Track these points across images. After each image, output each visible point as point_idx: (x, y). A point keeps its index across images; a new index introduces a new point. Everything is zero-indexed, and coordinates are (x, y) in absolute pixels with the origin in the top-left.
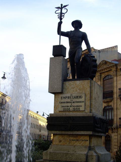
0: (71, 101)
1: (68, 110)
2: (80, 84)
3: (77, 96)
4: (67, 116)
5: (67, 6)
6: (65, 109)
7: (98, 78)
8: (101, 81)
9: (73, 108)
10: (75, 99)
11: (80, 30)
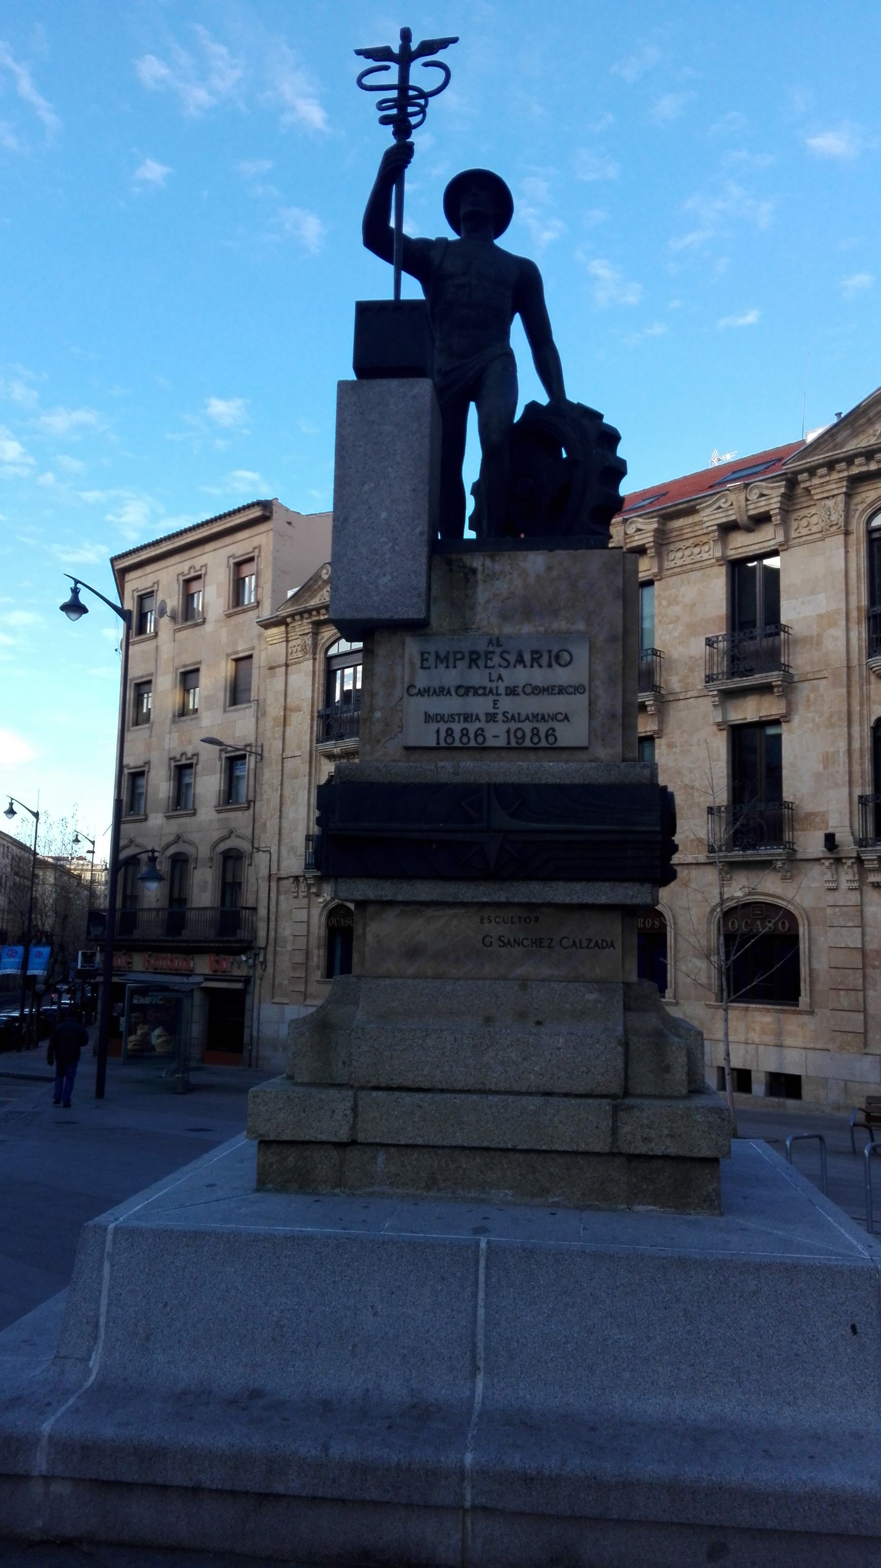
0: (493, 685)
1: (473, 744)
2: (555, 573)
3: (534, 652)
4: (471, 779)
7: (304, 649)
8: (314, 659)
9: (504, 727)
10: (520, 667)
11: (500, 242)
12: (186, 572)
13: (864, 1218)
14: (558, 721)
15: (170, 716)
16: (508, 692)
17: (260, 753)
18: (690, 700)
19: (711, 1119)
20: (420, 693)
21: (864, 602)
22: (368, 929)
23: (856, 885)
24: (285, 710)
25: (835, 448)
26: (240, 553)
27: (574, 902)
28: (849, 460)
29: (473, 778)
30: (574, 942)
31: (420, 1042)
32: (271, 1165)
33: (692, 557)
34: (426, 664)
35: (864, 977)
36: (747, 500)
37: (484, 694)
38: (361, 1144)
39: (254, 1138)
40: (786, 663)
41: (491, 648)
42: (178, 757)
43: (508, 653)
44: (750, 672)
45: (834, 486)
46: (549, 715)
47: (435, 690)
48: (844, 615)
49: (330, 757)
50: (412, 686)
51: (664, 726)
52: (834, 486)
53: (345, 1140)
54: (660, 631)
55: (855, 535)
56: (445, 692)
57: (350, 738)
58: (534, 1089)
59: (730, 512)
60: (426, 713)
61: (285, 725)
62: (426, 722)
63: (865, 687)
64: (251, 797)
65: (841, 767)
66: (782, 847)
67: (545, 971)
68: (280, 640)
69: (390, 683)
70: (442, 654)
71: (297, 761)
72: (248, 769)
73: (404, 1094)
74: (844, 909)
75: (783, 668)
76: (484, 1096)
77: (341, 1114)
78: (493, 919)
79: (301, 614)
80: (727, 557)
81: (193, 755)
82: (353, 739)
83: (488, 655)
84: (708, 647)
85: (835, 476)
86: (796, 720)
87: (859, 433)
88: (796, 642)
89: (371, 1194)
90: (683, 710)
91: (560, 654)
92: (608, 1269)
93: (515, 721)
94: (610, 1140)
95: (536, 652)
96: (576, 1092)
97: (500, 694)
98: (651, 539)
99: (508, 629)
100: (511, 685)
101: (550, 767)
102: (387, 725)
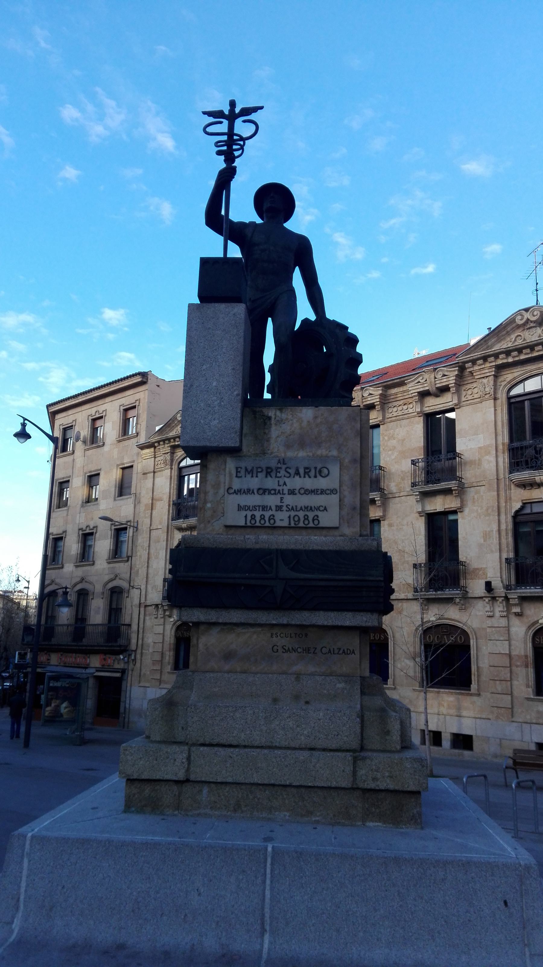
0: (281, 488)
1: (267, 524)
2: (319, 420)
3: (306, 468)
5: (256, 109)
6: (253, 517)
7: (165, 462)
8: (171, 469)
9: (288, 514)
10: (297, 477)
11: (287, 225)
12: (93, 414)
13: (513, 828)
14: (320, 511)
15: (80, 503)
16: (290, 493)
17: (136, 526)
18: (402, 498)
19: (415, 766)
20: (235, 492)
21: (507, 440)
22: (200, 641)
23: (505, 614)
24: (152, 499)
25: (488, 348)
26: (127, 403)
27: (329, 624)
28: (496, 356)
29: (267, 545)
30: (330, 650)
31: (232, 714)
32: (134, 795)
33: (402, 411)
34: (239, 475)
35: (511, 672)
36: (435, 378)
37: (275, 494)
38: (192, 781)
39: (124, 777)
40: (460, 476)
41: (279, 465)
42: (84, 528)
43: (290, 468)
44: (438, 481)
45: (487, 371)
46: (315, 507)
47: (244, 490)
48: (495, 448)
49: (180, 529)
50: (230, 488)
51: (387, 512)
52: (487, 371)
53: (182, 779)
54: (384, 455)
55: (500, 400)
56: (251, 492)
57: (192, 518)
58: (304, 746)
59: (425, 385)
60: (239, 505)
61: (152, 509)
62: (238, 510)
63: (508, 492)
64: (129, 554)
65: (495, 540)
66: (459, 589)
67: (311, 669)
68: (151, 457)
69: (217, 486)
70: (249, 468)
71: (160, 531)
72: (128, 537)
73: (220, 749)
74: (498, 629)
75: (458, 479)
76: (272, 750)
77: (180, 761)
78: (278, 635)
79: (164, 441)
80: (424, 411)
81: (94, 527)
82: (194, 519)
83: (278, 469)
84: (412, 465)
85: (488, 365)
86: (467, 511)
87: (502, 340)
88: (466, 463)
89: (199, 815)
90: (398, 504)
91: (322, 469)
92: (350, 865)
93: (294, 511)
94: (352, 779)
95: (307, 468)
96: (330, 748)
97: (285, 494)
98: (378, 400)
99: (290, 454)
100: (292, 488)
101: (315, 539)
102: (214, 512)
